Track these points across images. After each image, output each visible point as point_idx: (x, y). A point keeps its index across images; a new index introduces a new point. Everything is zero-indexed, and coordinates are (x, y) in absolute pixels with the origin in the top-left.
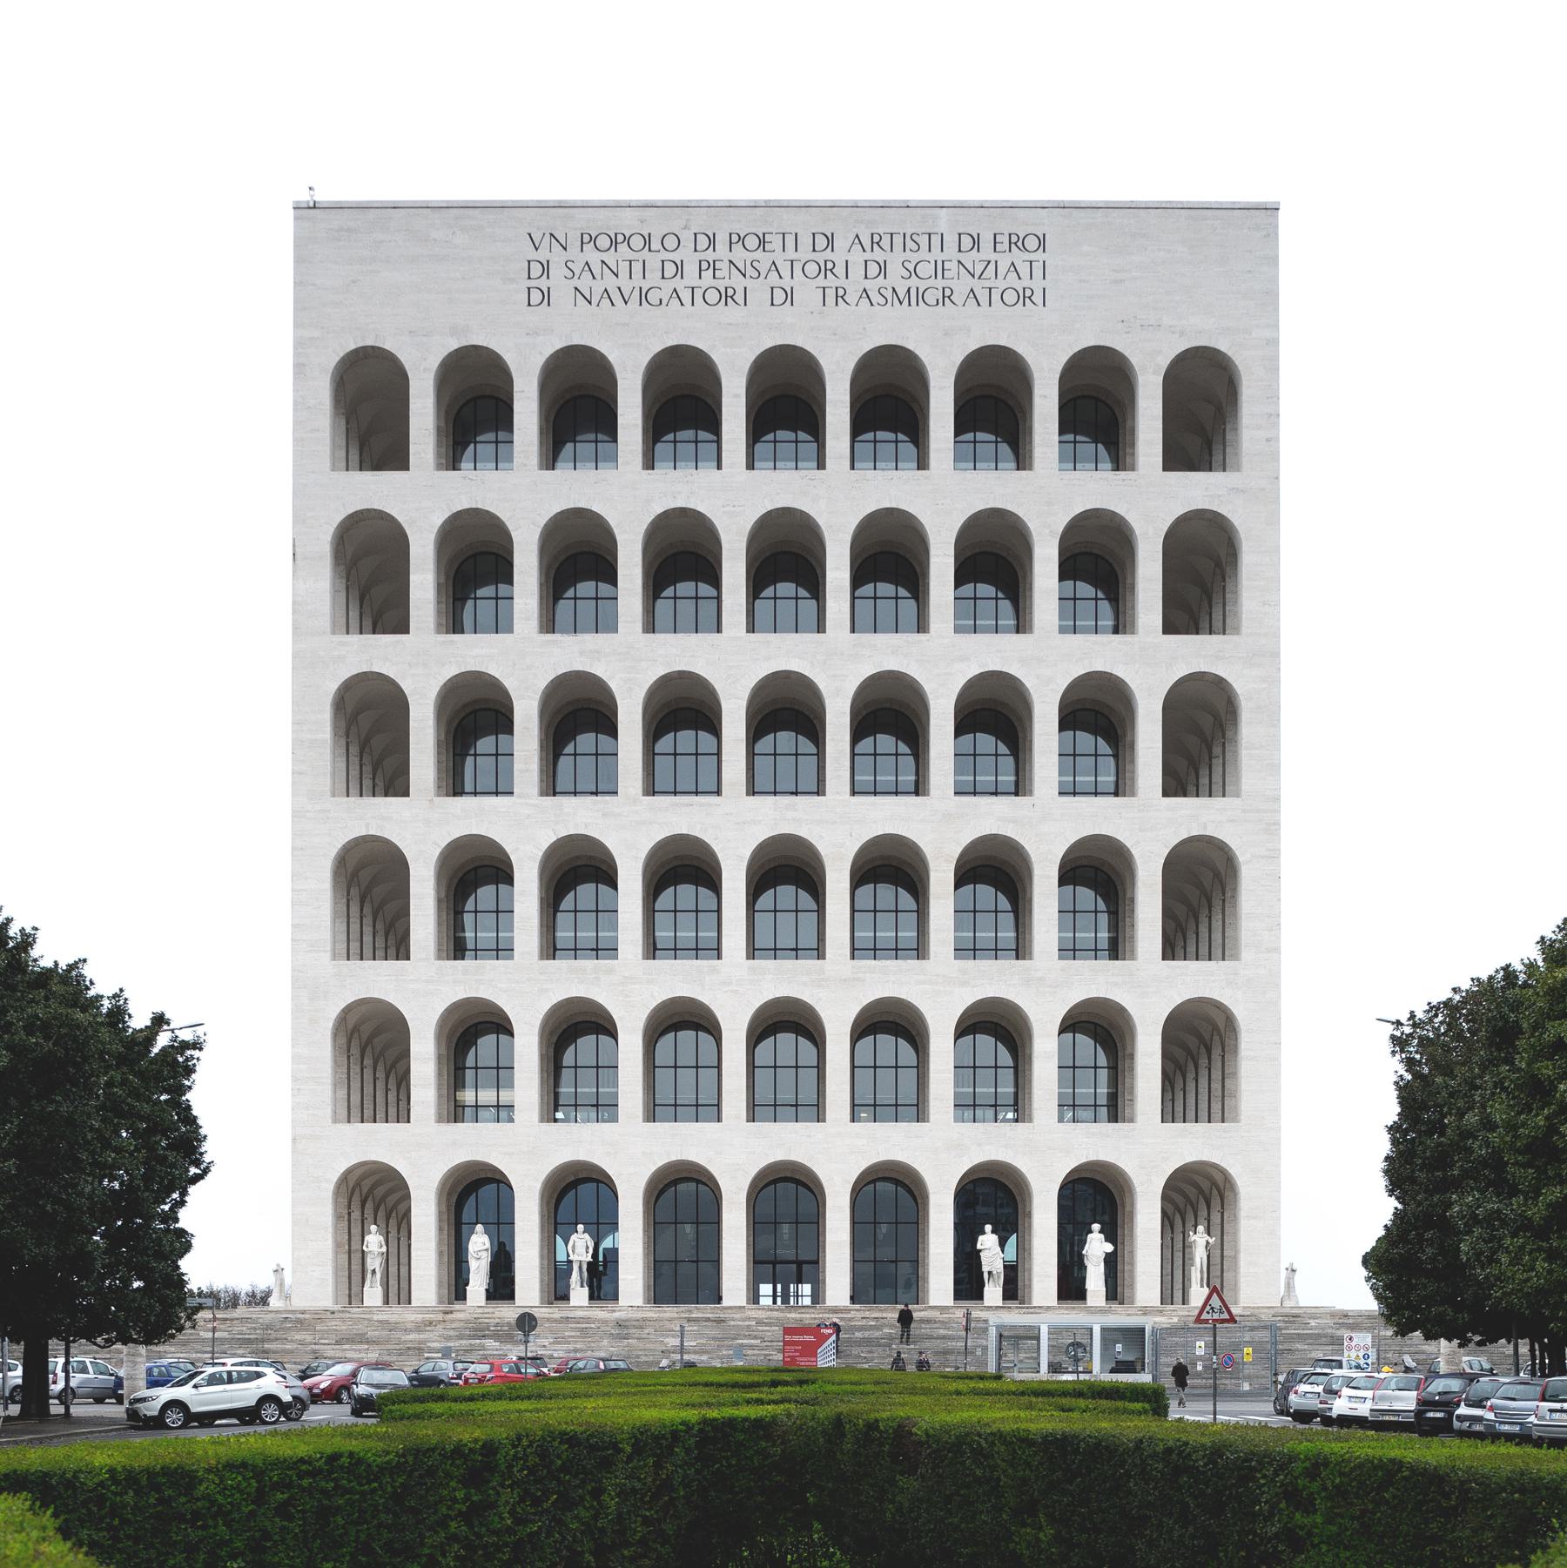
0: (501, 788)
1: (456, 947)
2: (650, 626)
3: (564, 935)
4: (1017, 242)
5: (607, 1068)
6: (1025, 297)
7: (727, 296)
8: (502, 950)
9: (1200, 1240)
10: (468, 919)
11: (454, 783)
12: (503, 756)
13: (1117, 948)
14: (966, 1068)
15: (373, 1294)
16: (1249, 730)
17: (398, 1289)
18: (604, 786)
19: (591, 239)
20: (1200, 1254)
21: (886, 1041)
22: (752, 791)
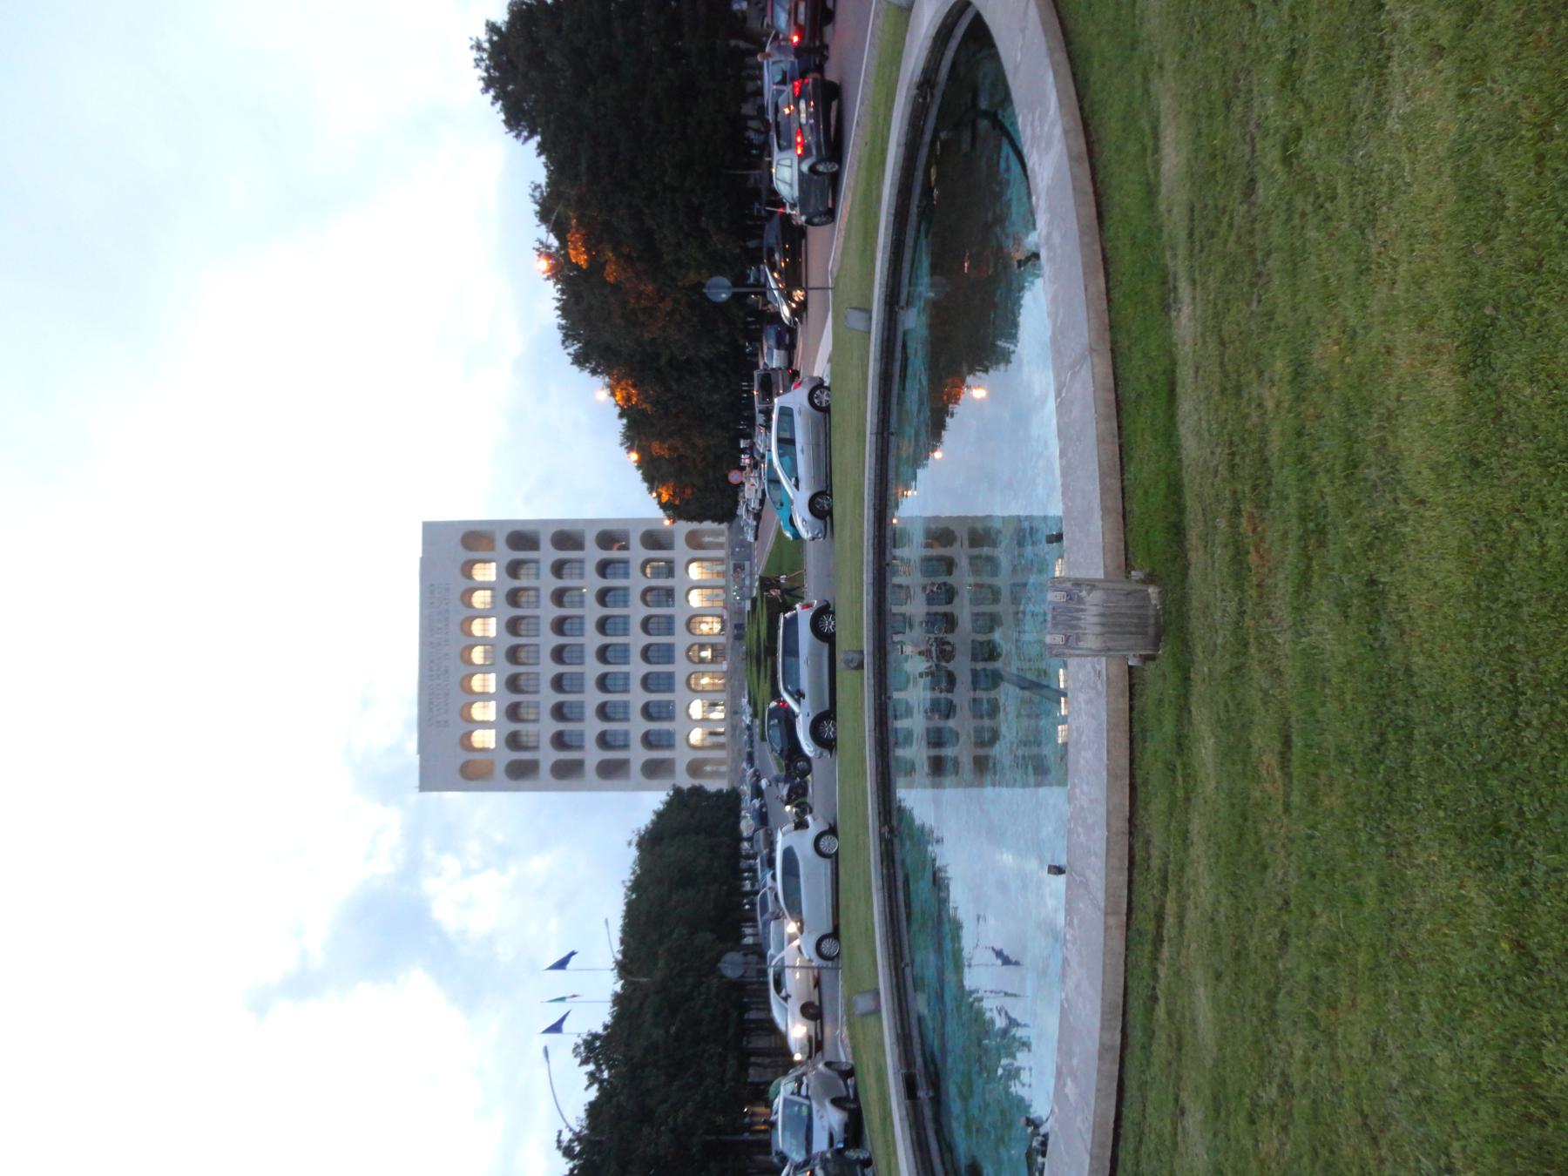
0: (581, 734)
1: (626, 746)
2: (537, 692)
3: (621, 716)
4: (432, 592)
5: (659, 704)
6: (447, 589)
7: (446, 672)
8: (626, 734)
9: (706, 539)
10: (618, 743)
11: (580, 747)
12: (572, 733)
13: (626, 562)
14: (659, 604)
15: (723, 769)
16: (566, 528)
17: (720, 762)
18: (581, 705)
19: (431, 710)
20: (711, 539)
21: (650, 626)
22: (582, 663)
